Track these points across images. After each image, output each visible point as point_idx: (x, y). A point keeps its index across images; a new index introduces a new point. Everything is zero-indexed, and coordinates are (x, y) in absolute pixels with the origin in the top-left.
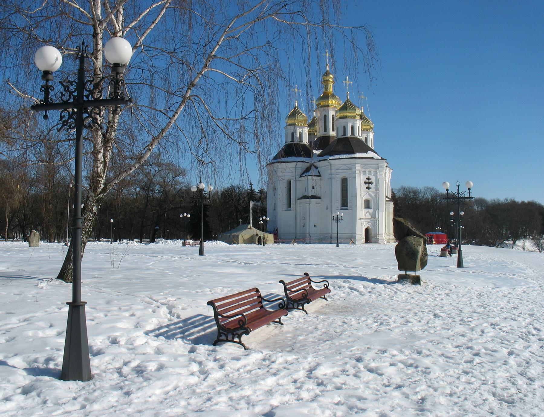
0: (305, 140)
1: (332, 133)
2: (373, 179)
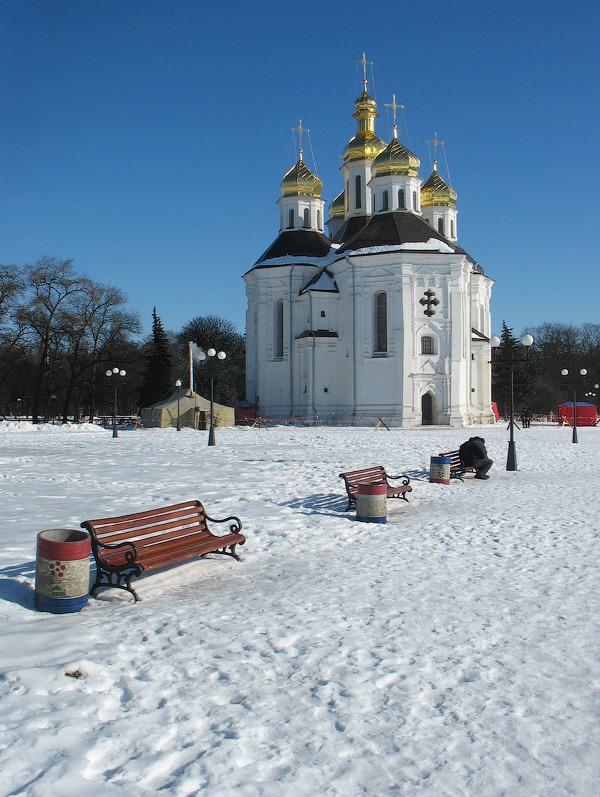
0: (317, 225)
1: (369, 211)
2: (438, 295)
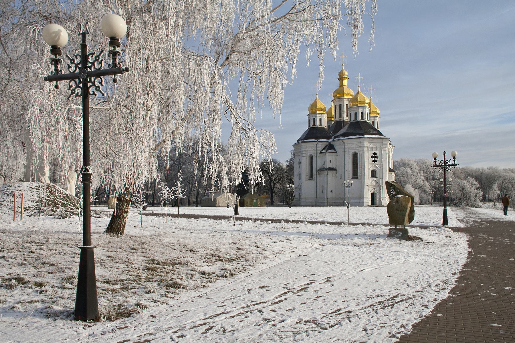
0: (325, 124)
1: (345, 118)
2: (378, 155)
